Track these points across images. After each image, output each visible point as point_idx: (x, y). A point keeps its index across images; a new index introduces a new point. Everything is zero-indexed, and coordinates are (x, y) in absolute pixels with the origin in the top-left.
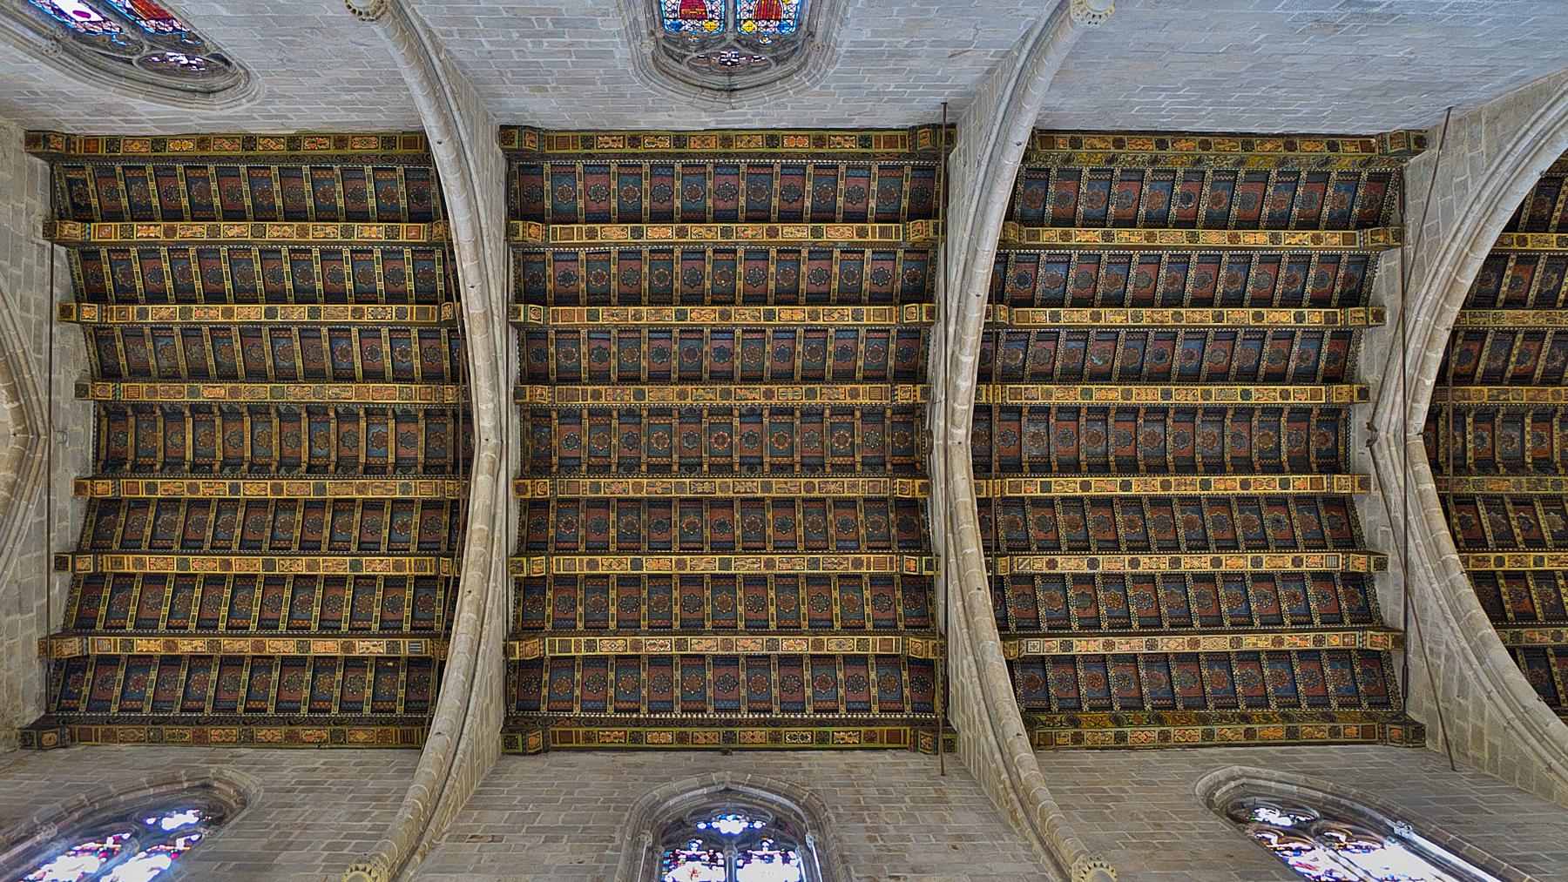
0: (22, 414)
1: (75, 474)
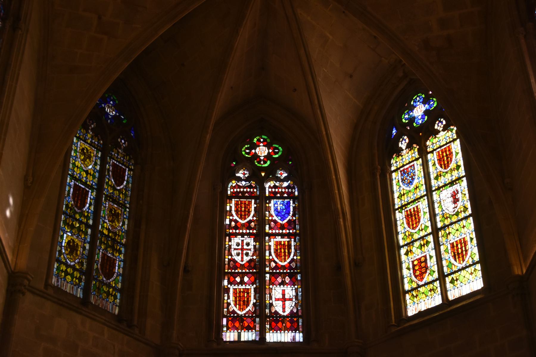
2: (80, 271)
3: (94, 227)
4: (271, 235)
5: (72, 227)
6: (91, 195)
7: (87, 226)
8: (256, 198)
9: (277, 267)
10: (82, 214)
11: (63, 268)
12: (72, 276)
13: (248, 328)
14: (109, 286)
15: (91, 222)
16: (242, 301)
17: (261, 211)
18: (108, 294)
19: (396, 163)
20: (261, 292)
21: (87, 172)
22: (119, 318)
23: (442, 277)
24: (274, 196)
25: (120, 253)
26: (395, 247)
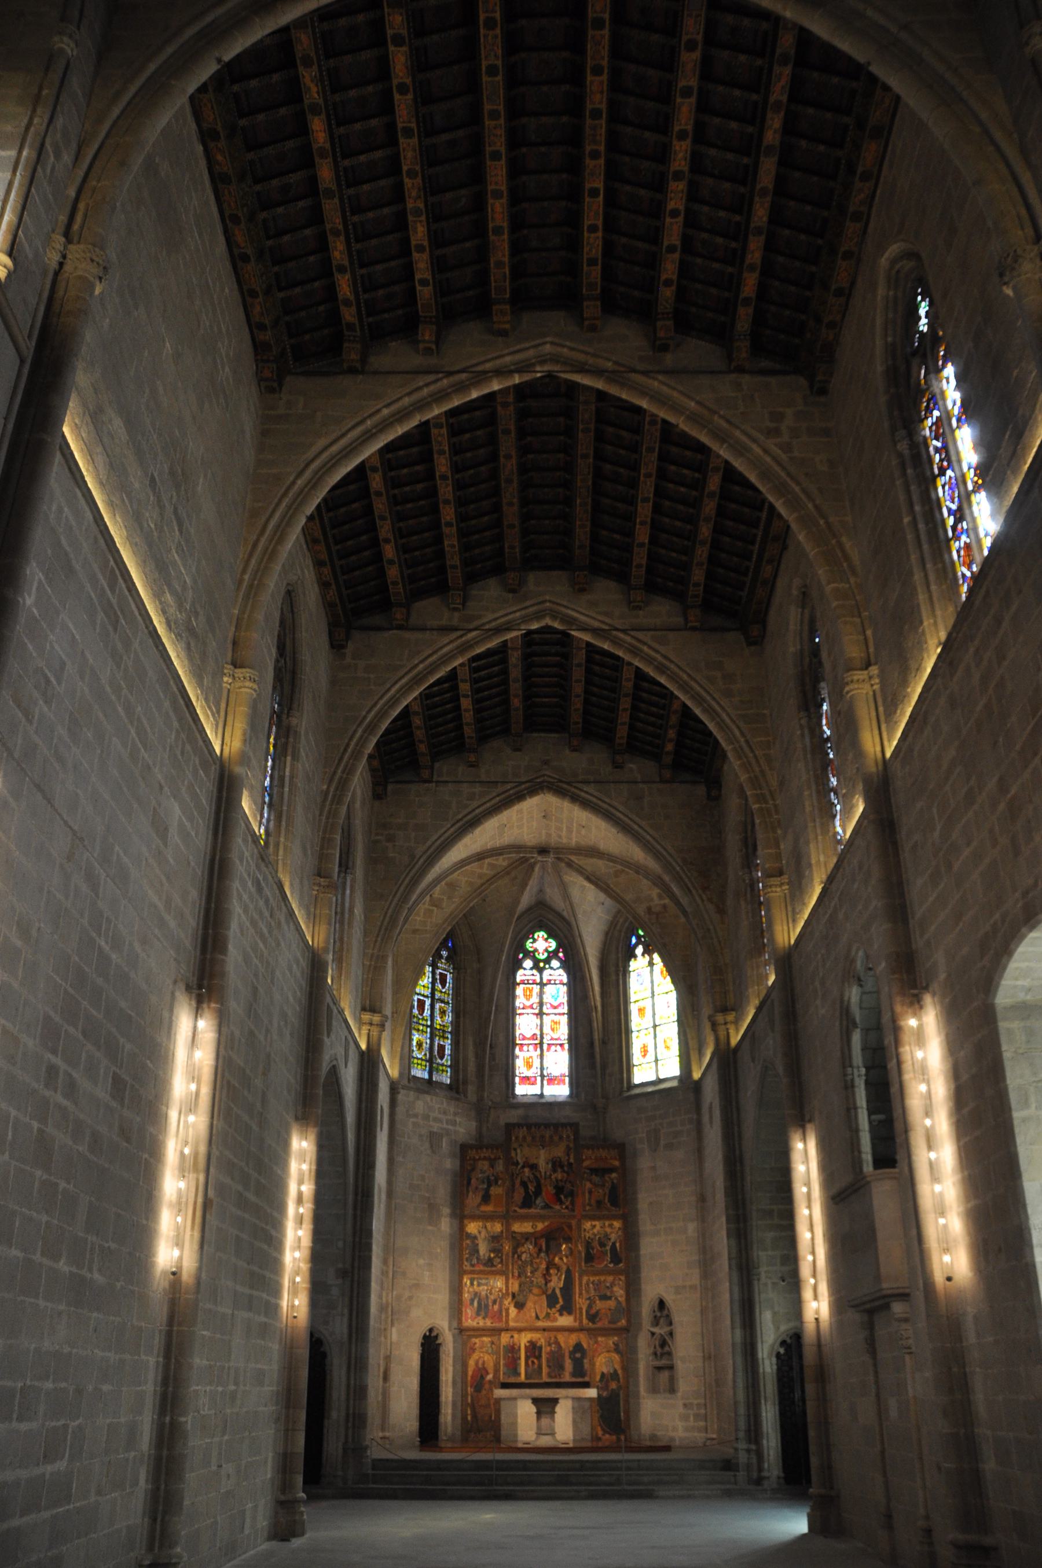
0: (533, 792)
1: (567, 752)
2: (426, 1061)
3: (432, 1026)
4: (547, 1014)
5: (418, 1030)
6: (428, 1002)
7: (427, 1026)
8: (537, 984)
9: (552, 1039)
10: (423, 1019)
11: (416, 1061)
12: (421, 1065)
13: (534, 1083)
14: (443, 1065)
15: (429, 1023)
16: (529, 1065)
17: (541, 994)
18: (443, 1071)
19: (633, 964)
20: (542, 1056)
21: (424, 986)
22: (450, 1087)
23: (656, 1060)
24: (549, 982)
25: (447, 1038)
26: (628, 1032)
